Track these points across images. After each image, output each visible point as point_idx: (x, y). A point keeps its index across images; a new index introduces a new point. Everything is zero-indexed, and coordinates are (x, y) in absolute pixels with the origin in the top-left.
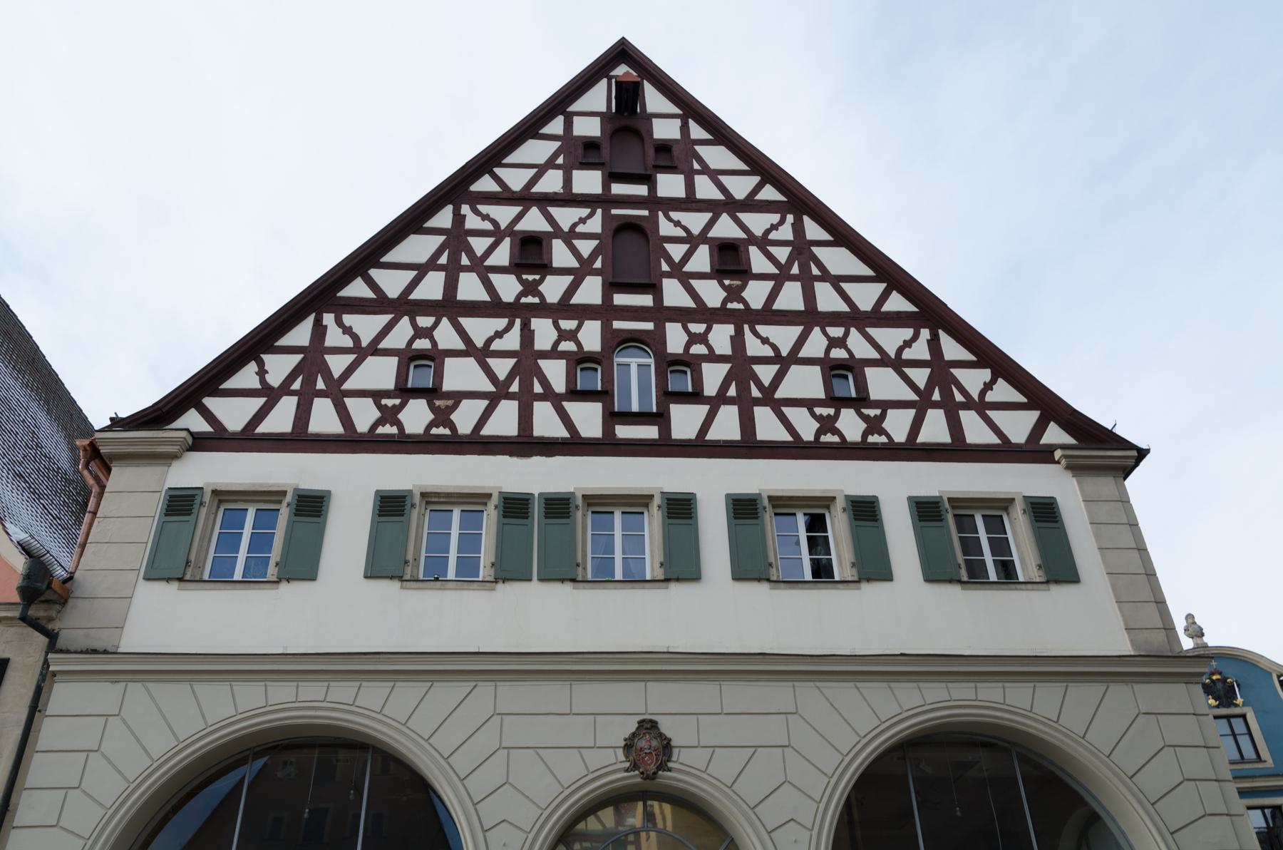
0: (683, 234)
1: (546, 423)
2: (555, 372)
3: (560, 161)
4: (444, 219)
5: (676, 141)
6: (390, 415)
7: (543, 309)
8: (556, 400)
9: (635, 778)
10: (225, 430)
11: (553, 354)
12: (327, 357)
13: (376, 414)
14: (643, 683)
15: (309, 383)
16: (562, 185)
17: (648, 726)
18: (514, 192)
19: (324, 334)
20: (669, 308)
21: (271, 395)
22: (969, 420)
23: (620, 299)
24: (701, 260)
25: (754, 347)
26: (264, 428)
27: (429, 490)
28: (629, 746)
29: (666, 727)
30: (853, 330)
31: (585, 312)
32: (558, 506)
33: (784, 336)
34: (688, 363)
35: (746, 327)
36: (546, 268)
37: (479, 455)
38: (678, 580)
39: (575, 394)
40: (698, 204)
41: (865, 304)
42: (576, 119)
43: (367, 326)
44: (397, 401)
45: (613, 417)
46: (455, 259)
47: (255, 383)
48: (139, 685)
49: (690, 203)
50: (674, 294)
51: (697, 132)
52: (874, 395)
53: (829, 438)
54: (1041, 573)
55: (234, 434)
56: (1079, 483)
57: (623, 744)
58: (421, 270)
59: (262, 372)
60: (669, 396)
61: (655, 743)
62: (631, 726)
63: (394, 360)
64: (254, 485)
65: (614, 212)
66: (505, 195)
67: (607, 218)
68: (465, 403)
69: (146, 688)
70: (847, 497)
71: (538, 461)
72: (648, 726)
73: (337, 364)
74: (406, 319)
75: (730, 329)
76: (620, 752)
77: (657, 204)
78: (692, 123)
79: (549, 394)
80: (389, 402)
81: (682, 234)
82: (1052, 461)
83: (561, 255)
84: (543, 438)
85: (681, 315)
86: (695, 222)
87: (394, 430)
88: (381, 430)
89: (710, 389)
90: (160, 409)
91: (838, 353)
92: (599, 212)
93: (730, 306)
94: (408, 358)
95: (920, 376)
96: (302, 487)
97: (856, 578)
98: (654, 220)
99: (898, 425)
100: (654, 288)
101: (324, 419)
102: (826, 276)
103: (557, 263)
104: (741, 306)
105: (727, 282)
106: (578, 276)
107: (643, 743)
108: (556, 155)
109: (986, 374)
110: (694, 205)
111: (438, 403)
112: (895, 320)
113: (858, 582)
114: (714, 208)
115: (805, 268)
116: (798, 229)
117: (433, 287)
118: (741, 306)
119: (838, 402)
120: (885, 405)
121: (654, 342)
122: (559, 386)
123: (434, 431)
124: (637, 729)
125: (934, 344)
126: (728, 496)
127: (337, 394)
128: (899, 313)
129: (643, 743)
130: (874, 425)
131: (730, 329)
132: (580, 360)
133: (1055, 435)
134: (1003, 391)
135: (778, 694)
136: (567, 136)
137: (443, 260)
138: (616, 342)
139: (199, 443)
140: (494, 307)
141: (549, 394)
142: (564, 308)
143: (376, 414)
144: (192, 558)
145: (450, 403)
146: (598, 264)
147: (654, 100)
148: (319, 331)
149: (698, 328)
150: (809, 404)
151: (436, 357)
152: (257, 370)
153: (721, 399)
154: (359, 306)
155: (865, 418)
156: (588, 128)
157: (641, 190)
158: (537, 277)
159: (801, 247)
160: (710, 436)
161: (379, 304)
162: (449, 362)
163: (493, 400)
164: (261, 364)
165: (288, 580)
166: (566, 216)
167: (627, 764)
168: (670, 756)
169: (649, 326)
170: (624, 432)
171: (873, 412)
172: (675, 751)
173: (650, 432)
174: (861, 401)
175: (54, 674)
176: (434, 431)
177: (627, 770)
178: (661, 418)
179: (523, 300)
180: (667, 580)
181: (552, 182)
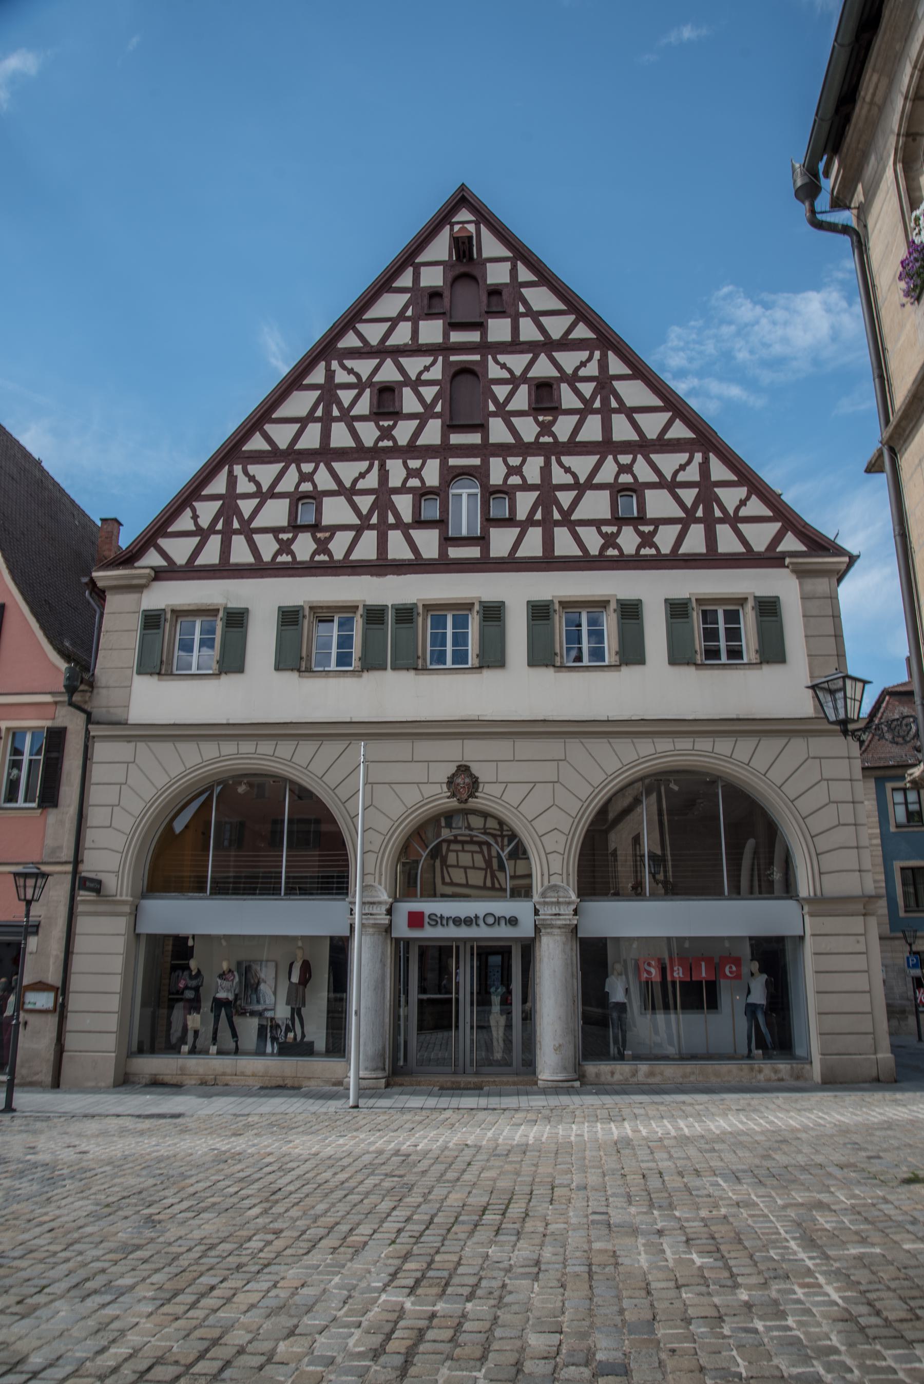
1: (398, 548)
2: (404, 504)
3: (409, 313)
4: (318, 376)
5: (506, 285)
6: (285, 547)
7: (396, 451)
9: (454, 803)
10: (175, 564)
11: (403, 489)
12: (239, 502)
13: (276, 546)
15: (228, 523)
17: (463, 769)
18: (373, 346)
19: (236, 482)
20: (494, 445)
21: (203, 534)
22: (724, 532)
23: (456, 439)
24: (521, 399)
25: (559, 476)
26: (200, 561)
27: (315, 604)
28: (450, 782)
29: (476, 769)
30: (639, 457)
31: (428, 452)
32: (405, 614)
33: (582, 465)
34: (506, 491)
35: (553, 458)
36: (397, 415)
38: (488, 667)
39: (419, 523)
40: (522, 346)
41: (652, 433)
42: (423, 269)
43: (265, 473)
44: (290, 535)
45: (447, 541)
46: (328, 411)
47: (191, 527)
49: (515, 346)
50: (498, 432)
51: (525, 275)
52: (650, 514)
53: (611, 552)
54: (758, 656)
55: (181, 566)
56: (800, 584)
57: (446, 780)
59: (195, 517)
60: (489, 521)
61: (467, 780)
62: (452, 769)
63: (287, 501)
65: (452, 358)
67: (447, 364)
68: (338, 534)
69: (149, 747)
70: (618, 601)
74: (293, 466)
75: (539, 461)
76: (445, 786)
77: (486, 348)
78: (520, 265)
79: (399, 525)
80: (284, 536)
81: (506, 375)
82: (783, 566)
83: (410, 403)
84: (394, 560)
85: (503, 450)
86: (517, 362)
87: (289, 558)
88: (280, 559)
89: (522, 514)
90: (131, 551)
91: (626, 478)
92: (440, 359)
93: (542, 440)
94: (297, 499)
95: (689, 496)
96: (229, 606)
97: (618, 663)
98: (484, 363)
99: (665, 538)
100: (482, 428)
101: (241, 553)
102: (623, 409)
103: (406, 410)
104: (550, 440)
105: (541, 418)
106: (423, 419)
107: (460, 780)
108: (405, 308)
109: (742, 492)
110: (518, 347)
111: (319, 535)
112: (675, 446)
113: (620, 666)
114: (533, 348)
115: (605, 402)
116: (603, 365)
117: (311, 439)
118: (550, 440)
119: (618, 521)
120: (658, 522)
121: (480, 474)
122: (407, 517)
123: (317, 558)
127: (248, 532)
128: (678, 440)
129: (460, 780)
130: (647, 540)
131: (539, 461)
132: (422, 494)
133: (791, 543)
134: (755, 507)
135: (554, 748)
137: (319, 413)
138: (450, 476)
139: (159, 575)
140: (358, 452)
141: (399, 525)
142: (412, 450)
143: (276, 546)
144: (164, 659)
145: (327, 534)
146: (438, 409)
147: (491, 246)
148: (232, 481)
149: (514, 461)
150: (597, 524)
151: (317, 497)
153: (530, 522)
154: (259, 458)
155: (640, 534)
156: (433, 278)
157: (474, 336)
158: (391, 423)
159: (604, 383)
160: (520, 554)
161: (274, 455)
162: (326, 501)
163: (359, 530)
164: (194, 510)
165: (226, 673)
166: (413, 365)
167: (449, 794)
168: (478, 788)
169: (477, 461)
170: (455, 553)
171: (646, 529)
172: (481, 786)
173: (474, 552)
175: (94, 737)
176: (317, 558)
177: (448, 797)
178: (482, 540)
179: (381, 444)
181: (402, 335)
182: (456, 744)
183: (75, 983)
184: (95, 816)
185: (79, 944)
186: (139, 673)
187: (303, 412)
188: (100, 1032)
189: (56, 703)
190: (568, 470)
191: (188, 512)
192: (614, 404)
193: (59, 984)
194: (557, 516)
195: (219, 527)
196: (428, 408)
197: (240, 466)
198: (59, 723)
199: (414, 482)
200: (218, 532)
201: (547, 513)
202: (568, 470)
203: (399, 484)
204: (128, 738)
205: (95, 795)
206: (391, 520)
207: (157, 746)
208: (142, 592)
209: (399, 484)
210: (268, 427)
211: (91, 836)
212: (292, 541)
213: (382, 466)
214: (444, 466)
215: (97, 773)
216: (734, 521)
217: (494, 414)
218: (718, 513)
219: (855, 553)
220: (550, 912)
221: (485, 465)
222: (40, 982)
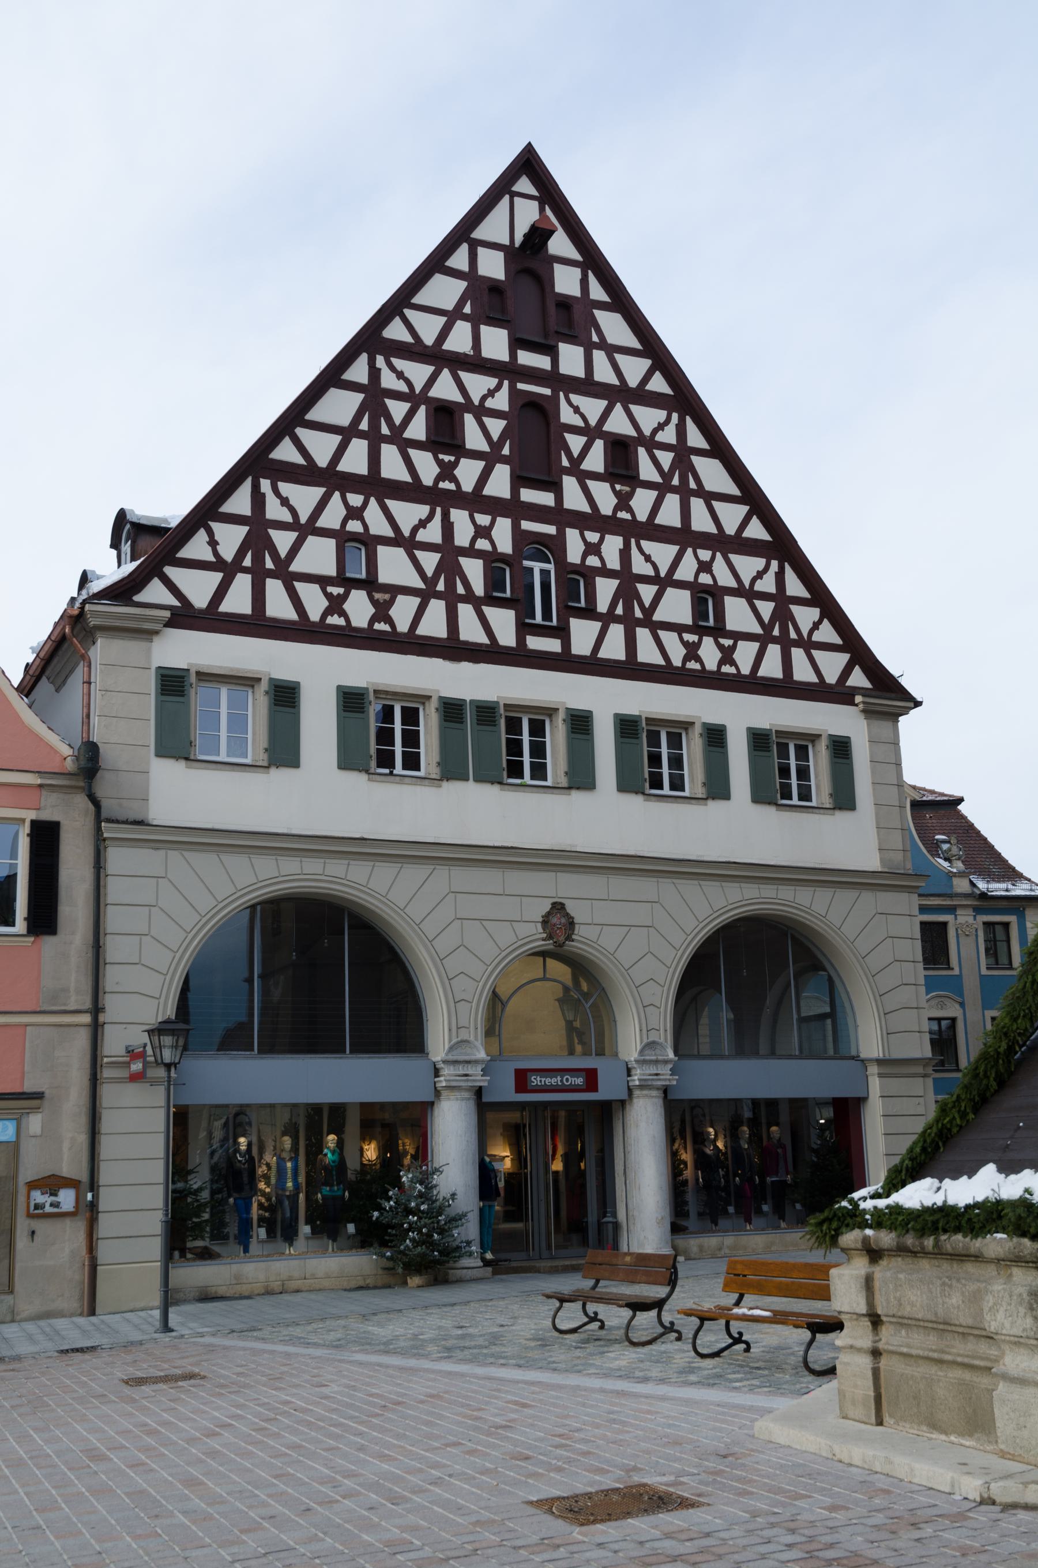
0: (581, 424)
2: (474, 570)
3: (467, 309)
6: (336, 605)
8: (477, 603)
9: (549, 945)
11: (471, 552)
12: (272, 532)
14: (554, 873)
15: (258, 560)
16: (471, 345)
17: (558, 907)
18: (426, 347)
21: (228, 570)
23: (528, 495)
24: (596, 460)
26: (226, 607)
27: (380, 689)
28: (545, 922)
29: (571, 908)
31: (496, 507)
32: (486, 712)
33: (663, 553)
35: (633, 541)
37: (418, 655)
38: (578, 788)
45: (524, 628)
47: (209, 556)
49: (588, 386)
51: (597, 292)
52: (730, 626)
54: (831, 801)
56: (868, 725)
57: (541, 920)
58: (347, 433)
59: (213, 543)
60: (569, 611)
61: (563, 920)
62: (547, 907)
64: (232, 669)
65: (521, 386)
66: (417, 349)
70: (704, 724)
71: (466, 667)
72: (559, 907)
73: (283, 541)
76: (539, 926)
79: (470, 597)
80: (336, 591)
82: (851, 703)
90: (134, 580)
91: (705, 579)
92: (506, 383)
97: (704, 796)
98: (554, 400)
100: (556, 487)
105: (618, 487)
107: (554, 920)
109: (814, 613)
112: (751, 548)
113: (706, 799)
121: (555, 547)
124: (551, 909)
125: (780, 577)
126: (616, 716)
128: (756, 540)
129: (554, 920)
132: (492, 560)
133: (858, 679)
134: (827, 633)
135: (647, 887)
136: (471, 276)
141: (470, 597)
143: (325, 603)
146: (506, 451)
148: (258, 500)
152: (208, 539)
159: (682, 452)
164: (210, 533)
166: (478, 384)
167: (545, 935)
168: (574, 931)
169: (551, 530)
171: (727, 642)
172: (577, 926)
173: (553, 645)
174: (719, 631)
177: (544, 940)
178: (562, 632)
180: (570, 788)
181: (459, 341)
182: (549, 876)
183: (105, 1177)
184: (115, 949)
185: (108, 1122)
186: (159, 755)
187: (344, 420)
189: (41, 786)
190: (648, 558)
191: (202, 535)
192: (693, 485)
193: (84, 1176)
194: (638, 614)
195: (247, 562)
196: (496, 446)
197: (268, 482)
198: (46, 816)
199: (482, 544)
200: (245, 570)
201: (629, 609)
202: (648, 558)
203: (466, 543)
204: (156, 845)
205: (114, 919)
206: (460, 590)
208: (151, 641)
209: (466, 543)
210: (301, 432)
211: (112, 977)
212: (345, 597)
213: (446, 516)
214: (516, 527)
215: (115, 890)
216: (809, 645)
217: (569, 472)
218: (793, 635)
219: (919, 699)
220: (648, 1072)
221: (561, 535)
222: (53, 1175)
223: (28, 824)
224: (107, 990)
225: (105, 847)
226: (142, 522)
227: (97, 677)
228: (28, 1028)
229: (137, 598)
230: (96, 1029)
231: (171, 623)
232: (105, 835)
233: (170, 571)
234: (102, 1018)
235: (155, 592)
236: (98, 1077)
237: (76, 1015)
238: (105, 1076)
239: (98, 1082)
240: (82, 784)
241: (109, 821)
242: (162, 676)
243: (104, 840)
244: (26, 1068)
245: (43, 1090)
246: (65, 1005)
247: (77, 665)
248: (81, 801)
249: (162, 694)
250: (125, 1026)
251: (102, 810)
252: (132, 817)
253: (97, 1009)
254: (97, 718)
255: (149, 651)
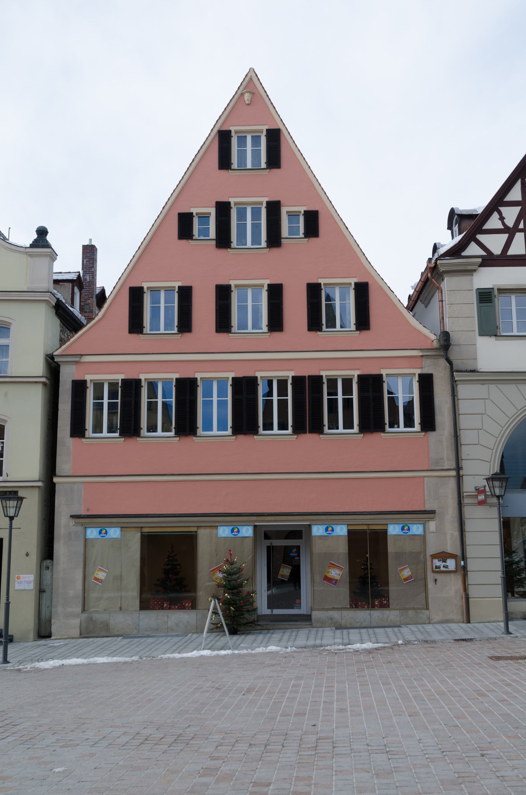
47: (500, 226)
48: (494, 385)
59: (502, 218)
64: (517, 285)
69: (497, 386)
90: (461, 244)
152: (499, 217)
164: (500, 213)
183: (470, 552)
184: (465, 437)
185: (469, 526)
186: (481, 335)
188: (485, 584)
189: (422, 356)
191: (496, 215)
193: (459, 553)
195: (521, 226)
198: (426, 371)
200: (521, 231)
205: (464, 422)
207: (505, 388)
211: (465, 451)
215: (463, 407)
222: (444, 552)
223: (417, 376)
224: (463, 458)
225: (457, 385)
226: (463, 213)
227: (446, 297)
228: (425, 478)
229: (463, 254)
230: (459, 478)
231: (482, 265)
232: (456, 379)
233: (480, 237)
234: (461, 473)
235: (473, 249)
236: (462, 503)
237: (448, 471)
238: (465, 502)
239: (462, 505)
240: (442, 353)
241: (457, 371)
242: (480, 293)
243: (456, 381)
244: (426, 498)
245: (435, 509)
246: (442, 466)
247: (435, 292)
248: (443, 362)
249: (480, 303)
250: (473, 476)
251: (454, 366)
252: (469, 368)
253: (458, 468)
254: (447, 319)
255: (471, 281)
